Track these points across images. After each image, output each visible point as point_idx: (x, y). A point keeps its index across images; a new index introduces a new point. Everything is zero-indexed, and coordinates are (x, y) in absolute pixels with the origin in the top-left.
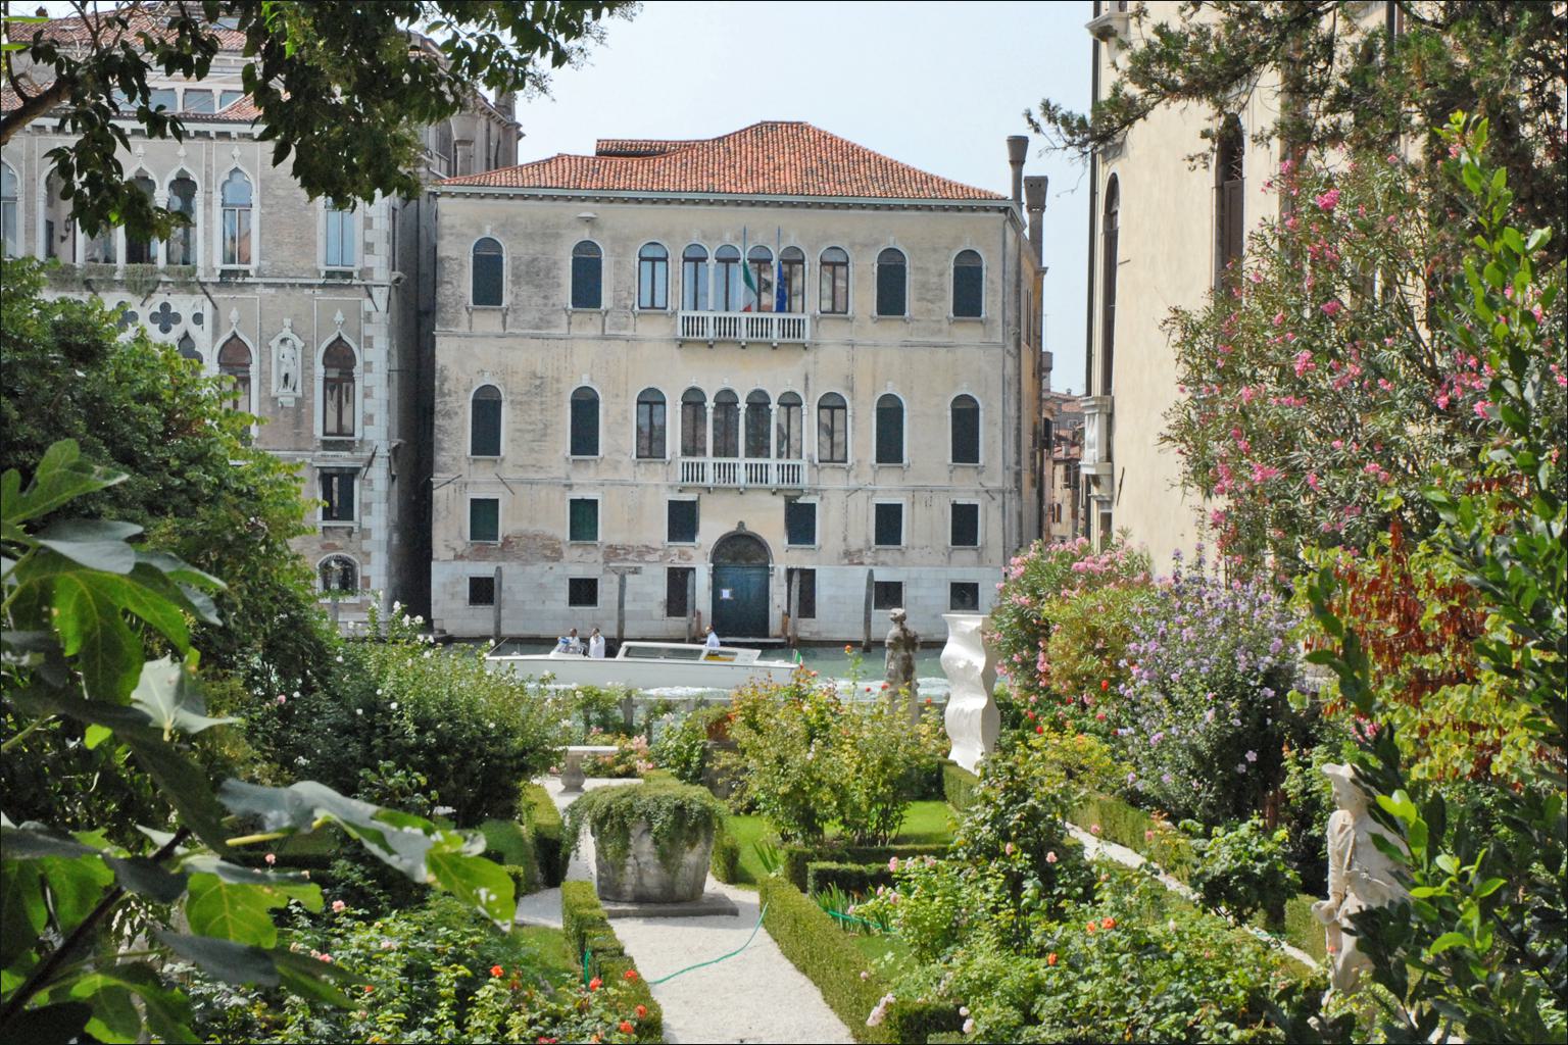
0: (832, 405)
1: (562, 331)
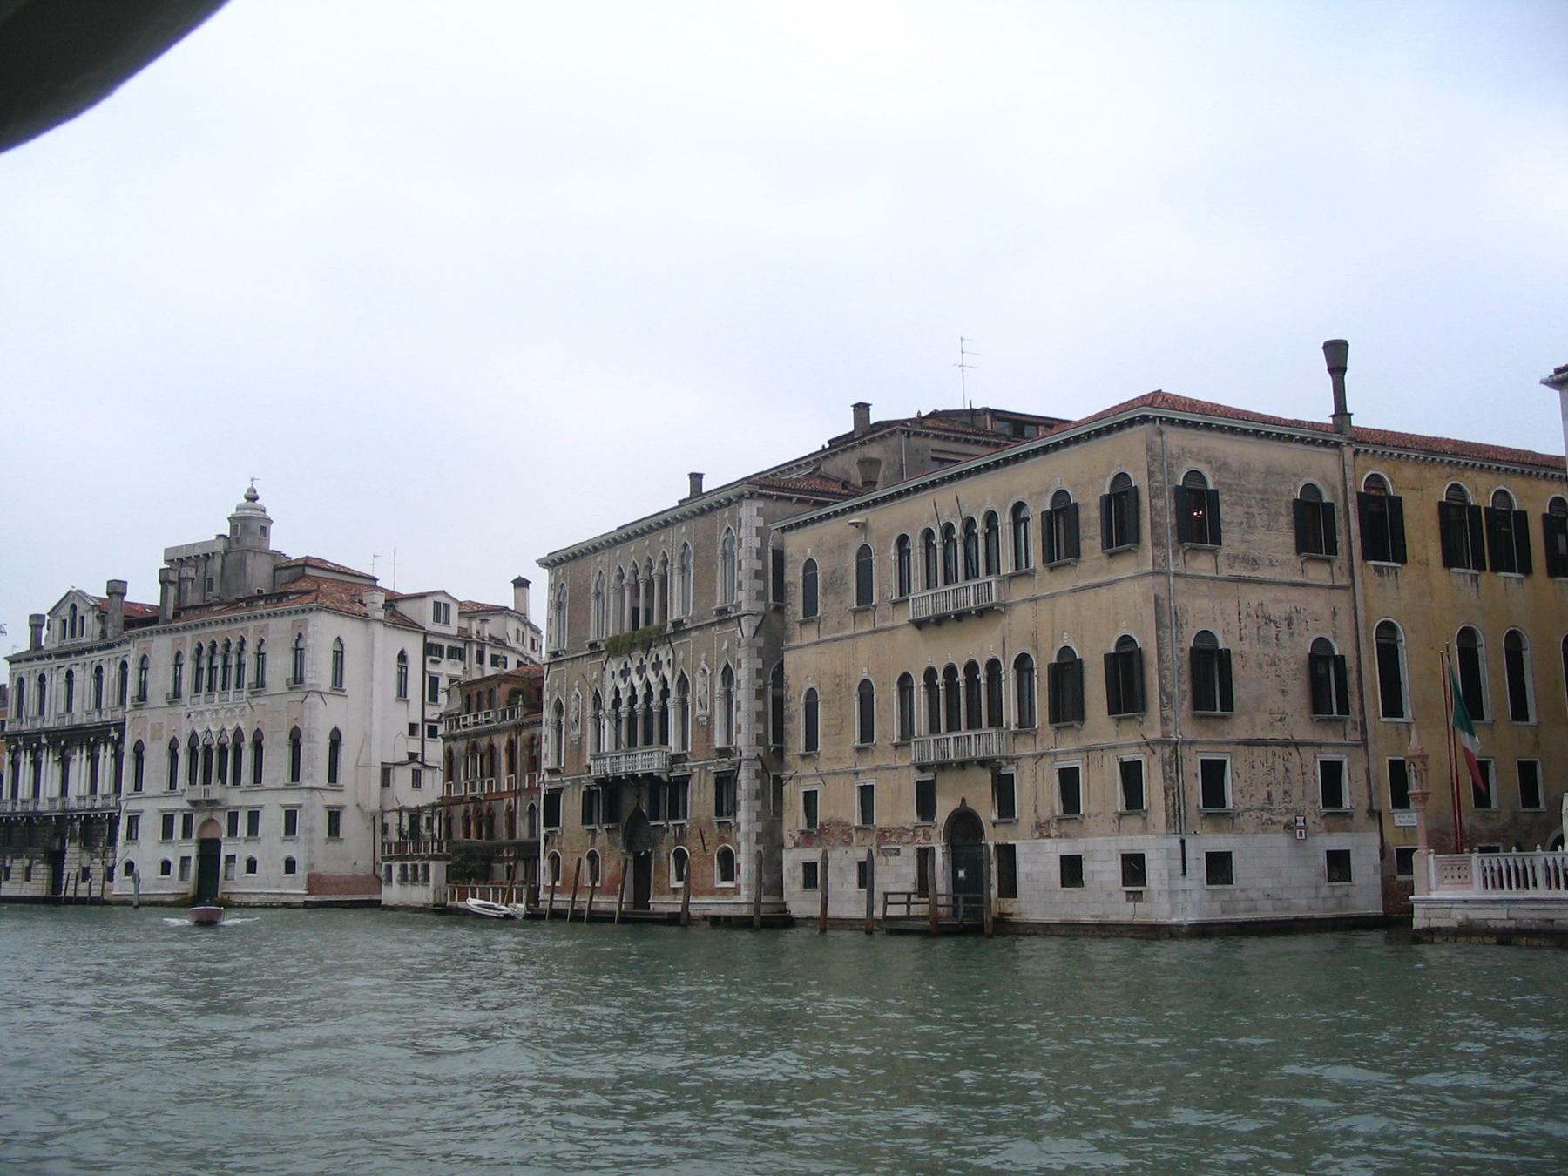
0: (1023, 663)
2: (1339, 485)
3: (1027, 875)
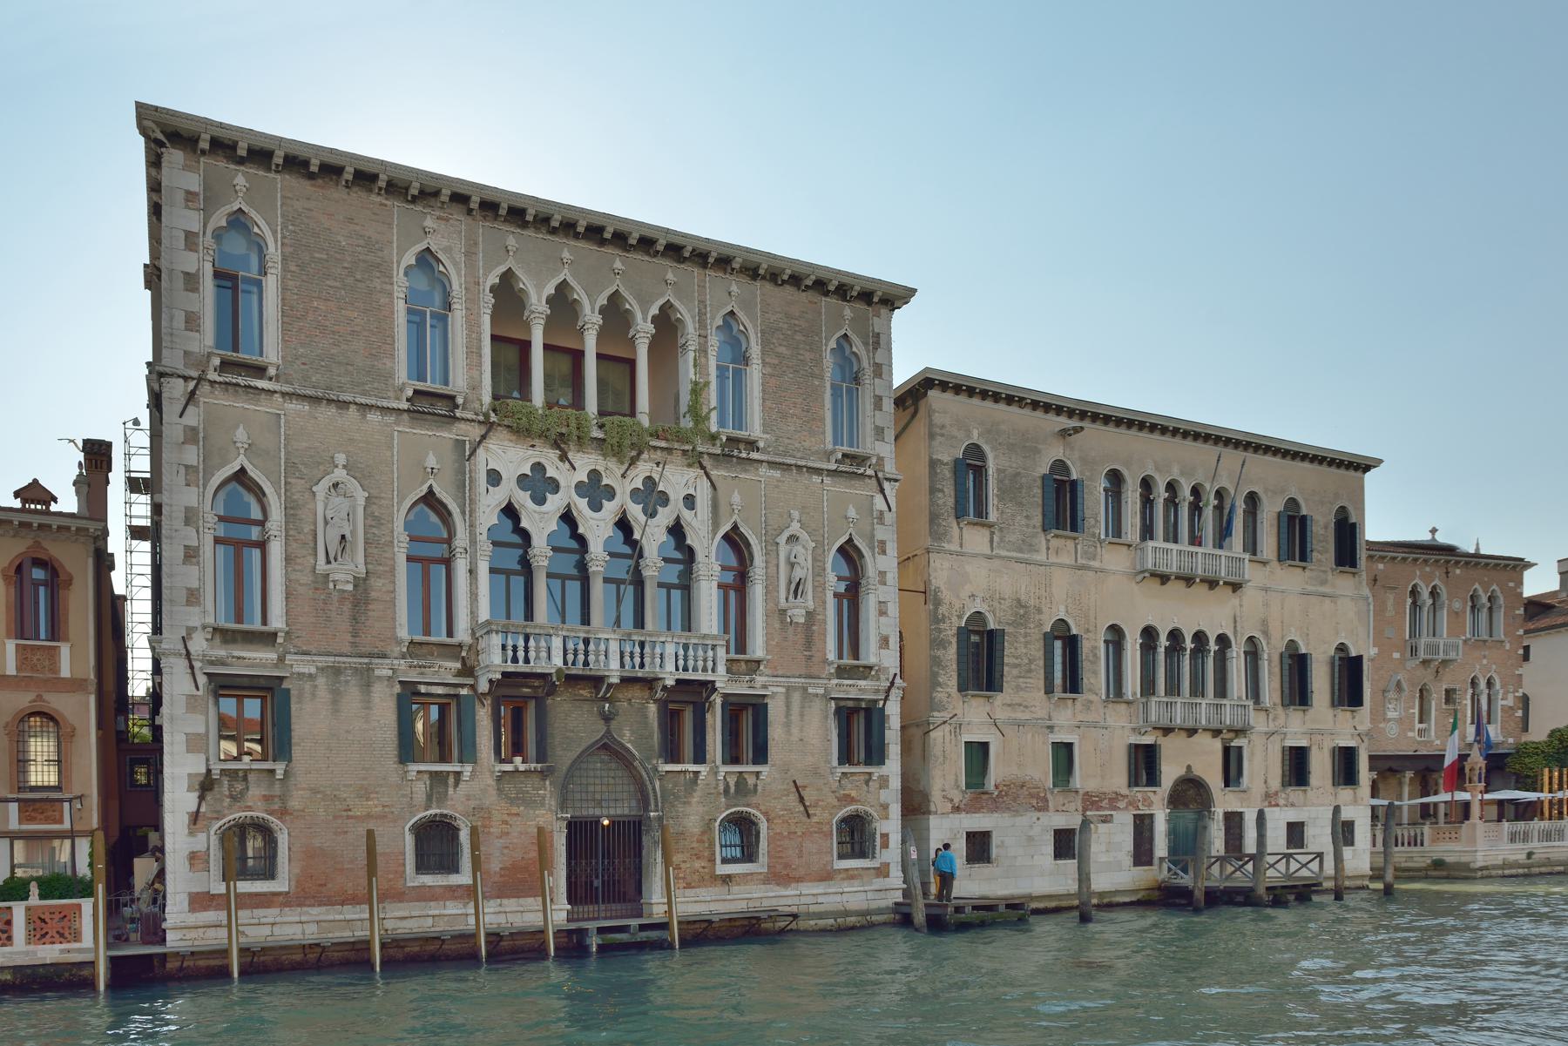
1: (1041, 557)
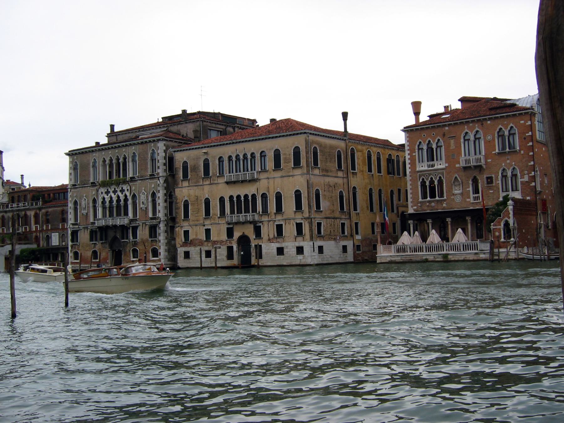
0: (264, 196)
1: (201, 183)
2: (345, 150)
3: (266, 253)
